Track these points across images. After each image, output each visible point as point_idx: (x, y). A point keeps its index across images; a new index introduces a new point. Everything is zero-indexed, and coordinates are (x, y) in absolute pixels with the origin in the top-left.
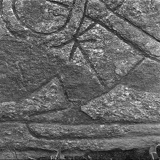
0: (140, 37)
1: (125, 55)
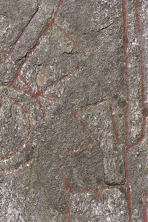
0: (32, 29)
1: (52, 43)
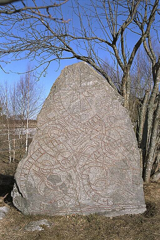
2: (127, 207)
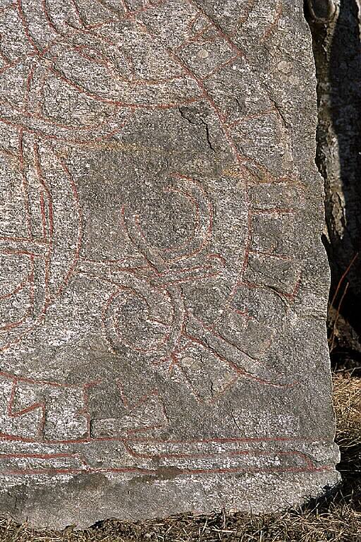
0: (236, 354)
2: (195, 456)
